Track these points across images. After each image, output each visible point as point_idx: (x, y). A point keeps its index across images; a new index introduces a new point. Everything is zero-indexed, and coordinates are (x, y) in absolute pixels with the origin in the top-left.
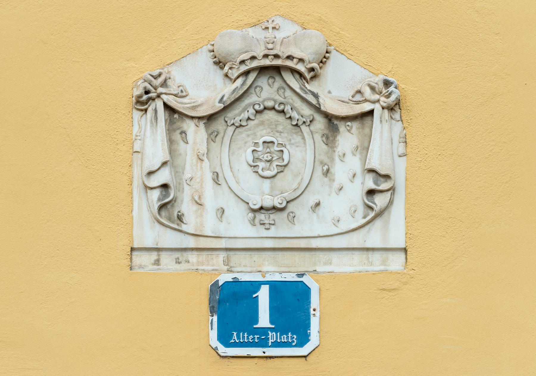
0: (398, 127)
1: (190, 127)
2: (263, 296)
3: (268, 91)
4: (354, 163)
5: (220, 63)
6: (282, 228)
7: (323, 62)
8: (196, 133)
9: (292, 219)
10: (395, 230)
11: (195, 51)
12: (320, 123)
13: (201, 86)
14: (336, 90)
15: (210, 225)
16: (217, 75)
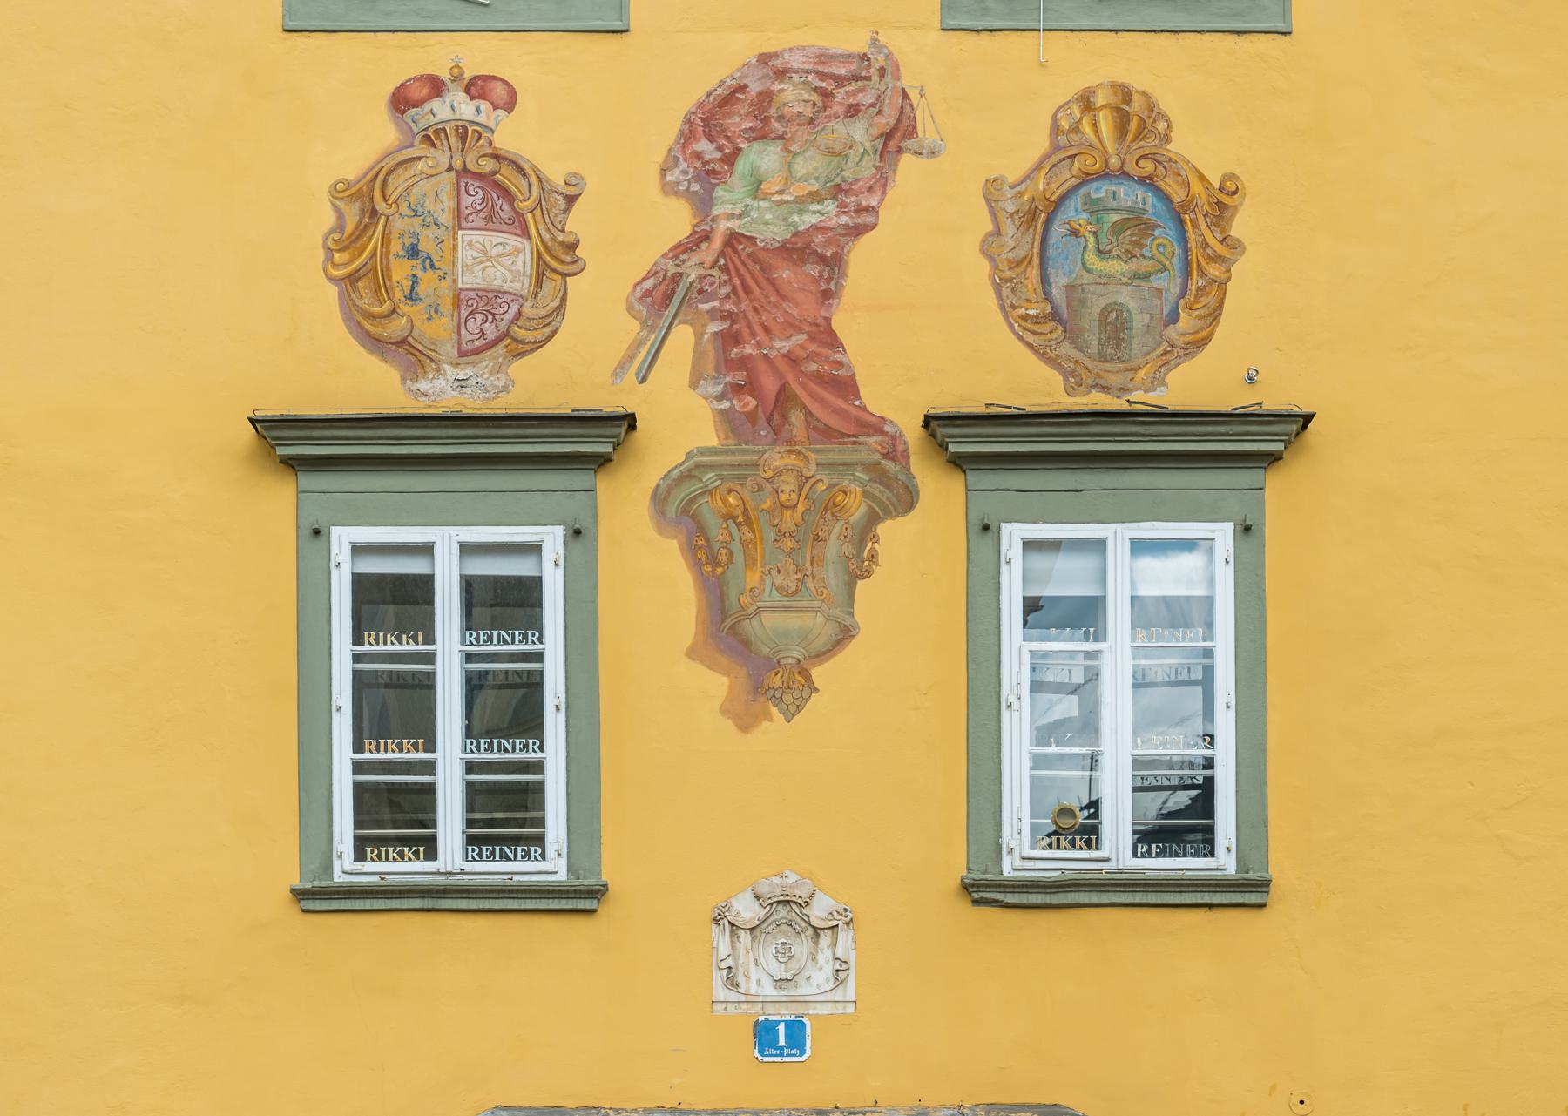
0: (851, 933)
1: (742, 933)
2: (782, 1028)
3: (782, 912)
4: (828, 953)
5: (758, 898)
6: (791, 992)
7: (811, 897)
8: (745, 937)
9: (796, 985)
10: (850, 991)
11: (744, 890)
12: (810, 931)
13: (747, 910)
15: (754, 989)
16: (755, 904)
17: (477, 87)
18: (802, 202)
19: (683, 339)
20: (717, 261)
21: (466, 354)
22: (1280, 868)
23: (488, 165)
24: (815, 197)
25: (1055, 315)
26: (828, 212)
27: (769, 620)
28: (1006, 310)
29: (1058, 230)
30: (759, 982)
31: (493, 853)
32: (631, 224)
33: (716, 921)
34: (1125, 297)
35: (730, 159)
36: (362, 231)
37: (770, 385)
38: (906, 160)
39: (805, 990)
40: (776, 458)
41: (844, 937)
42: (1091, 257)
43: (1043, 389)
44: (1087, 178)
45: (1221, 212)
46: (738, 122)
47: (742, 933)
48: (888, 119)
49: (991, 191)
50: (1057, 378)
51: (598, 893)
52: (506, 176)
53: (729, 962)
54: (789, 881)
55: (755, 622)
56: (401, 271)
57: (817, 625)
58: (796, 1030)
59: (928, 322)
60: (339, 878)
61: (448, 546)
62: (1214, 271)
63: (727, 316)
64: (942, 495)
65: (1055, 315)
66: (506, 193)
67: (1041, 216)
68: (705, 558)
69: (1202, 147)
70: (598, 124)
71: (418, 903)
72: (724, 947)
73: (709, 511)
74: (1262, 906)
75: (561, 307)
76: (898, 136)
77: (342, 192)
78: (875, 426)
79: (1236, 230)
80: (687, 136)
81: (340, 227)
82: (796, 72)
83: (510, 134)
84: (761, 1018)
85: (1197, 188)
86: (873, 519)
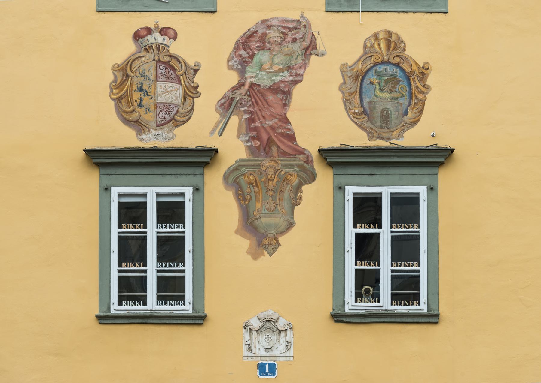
0: (292, 332)
1: (254, 332)
2: (267, 366)
3: (268, 324)
4: (284, 339)
5: (259, 319)
6: (271, 353)
7: (278, 319)
8: (255, 333)
9: (272, 350)
10: (291, 353)
11: (254, 316)
12: (278, 331)
13: (256, 324)
14: (281, 325)
15: (257, 352)
16: (258, 321)
17: (164, 31)
18: (276, 73)
19: (234, 120)
20: (247, 93)
21: (159, 126)
22: (443, 310)
23: (167, 59)
24: (281, 70)
25: (365, 112)
26: (286, 76)
27: (264, 220)
28: (347, 110)
29: (366, 82)
31: (166, 303)
32: (217, 80)
33: (245, 327)
34: (389, 106)
35: (252, 57)
36: (123, 82)
37: (265, 137)
38: (313, 57)
39: (275, 352)
40: (267, 163)
41: (289, 333)
42: (378, 92)
43: (359, 139)
44: (376, 64)
46: (254, 44)
47: (254, 332)
48: (306, 43)
49: (343, 68)
50: (365, 135)
51: (203, 317)
52: (174, 63)
53: (249, 342)
54: (270, 313)
55: (259, 221)
56: (136, 96)
58: (272, 367)
59: (321, 116)
60: (113, 312)
61: (152, 193)
62: (421, 96)
63: (251, 113)
64: (325, 177)
65: (365, 112)
66: (173, 69)
67: (360, 77)
68: (242, 198)
69: (416, 52)
70: (205, 44)
71: (140, 321)
72: (247, 337)
73: (243, 181)
74: (437, 323)
75: (192, 109)
76: (310, 49)
77: (116, 68)
78: (302, 152)
79: (429, 82)
81: (115, 80)
82: (275, 26)
83: (175, 48)
84: (261, 362)
85: (415, 67)
86: (300, 185)
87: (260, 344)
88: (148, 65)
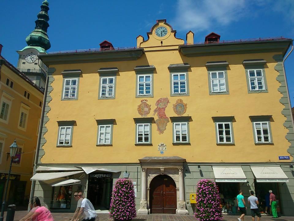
17: (145, 100)
18: (163, 106)
21: (145, 114)
25: (177, 111)
27: (161, 128)
30: (161, 149)
32: (154, 107)
35: (159, 104)
37: (161, 115)
39: (163, 149)
40: (162, 120)
43: (176, 116)
45: (186, 105)
46: (159, 102)
49: (173, 105)
50: (177, 115)
56: (141, 110)
57: (164, 129)
58: (163, 152)
69: (185, 102)
70: (152, 102)
76: (168, 102)
78: (167, 118)
79: (187, 106)
80: (157, 102)
83: (147, 103)
86: (167, 123)
87: (161, 148)
88: (143, 105)
